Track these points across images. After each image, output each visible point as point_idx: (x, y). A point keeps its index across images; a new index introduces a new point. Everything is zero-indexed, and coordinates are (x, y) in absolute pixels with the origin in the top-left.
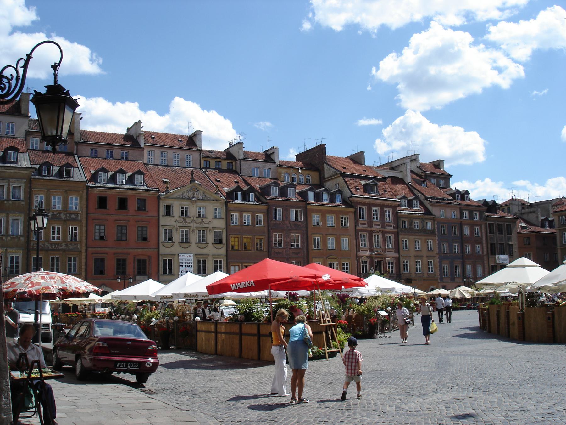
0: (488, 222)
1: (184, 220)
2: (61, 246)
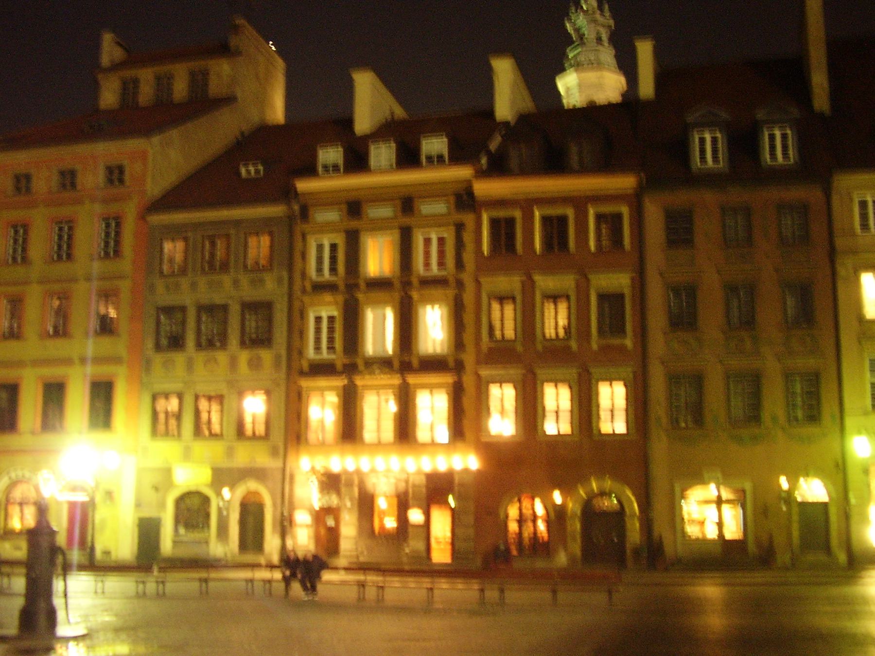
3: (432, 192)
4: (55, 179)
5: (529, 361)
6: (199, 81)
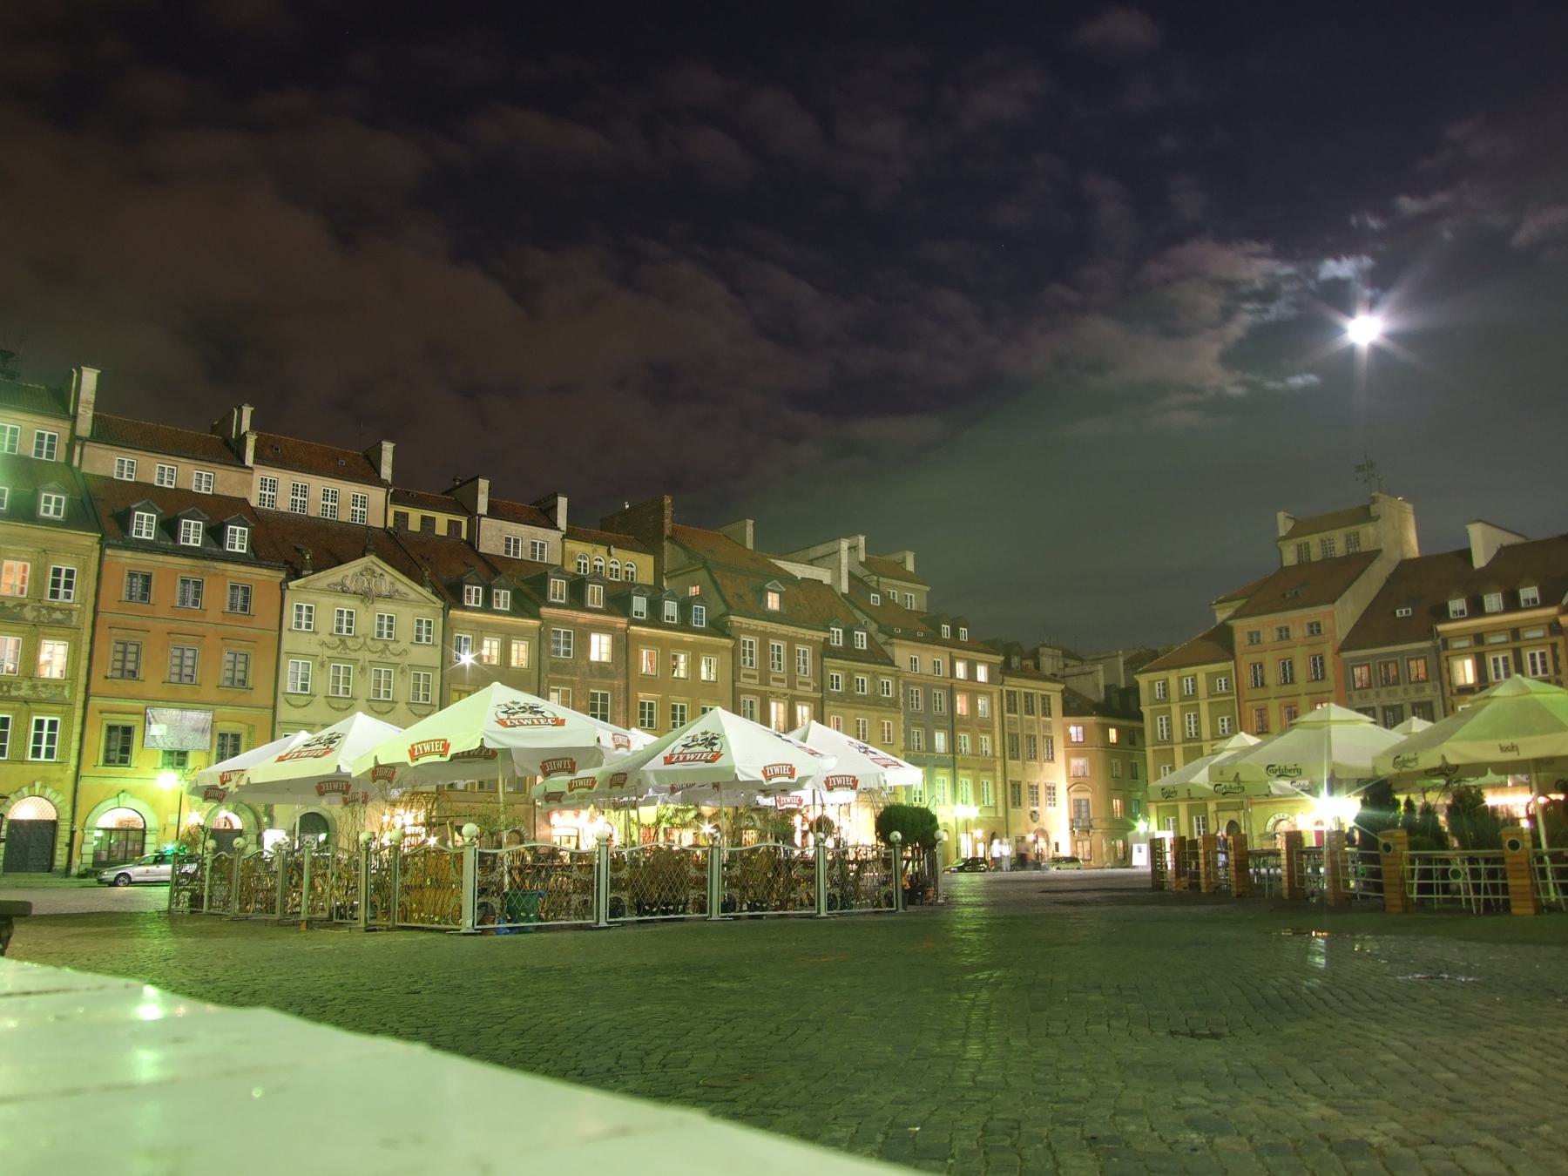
0: (1005, 689)
1: (343, 642)
2: (19, 689)
3: (1533, 624)
4: (1276, 635)
6: (1352, 540)
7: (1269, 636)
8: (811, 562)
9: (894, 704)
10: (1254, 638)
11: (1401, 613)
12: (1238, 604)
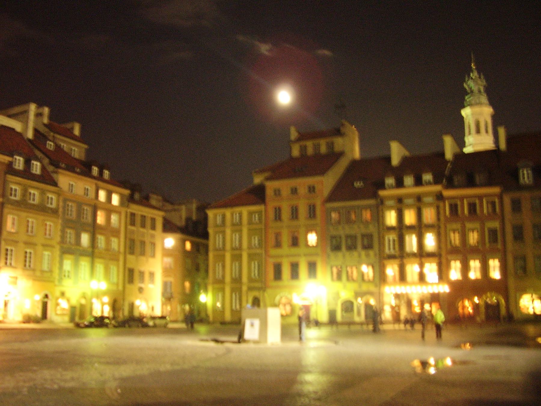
0: (129, 210)
3: (427, 194)
5: (464, 253)
6: (330, 146)
7: (286, 192)
8: (10, 116)
9: (55, 212)
10: (277, 193)
11: (358, 184)
12: (267, 174)
